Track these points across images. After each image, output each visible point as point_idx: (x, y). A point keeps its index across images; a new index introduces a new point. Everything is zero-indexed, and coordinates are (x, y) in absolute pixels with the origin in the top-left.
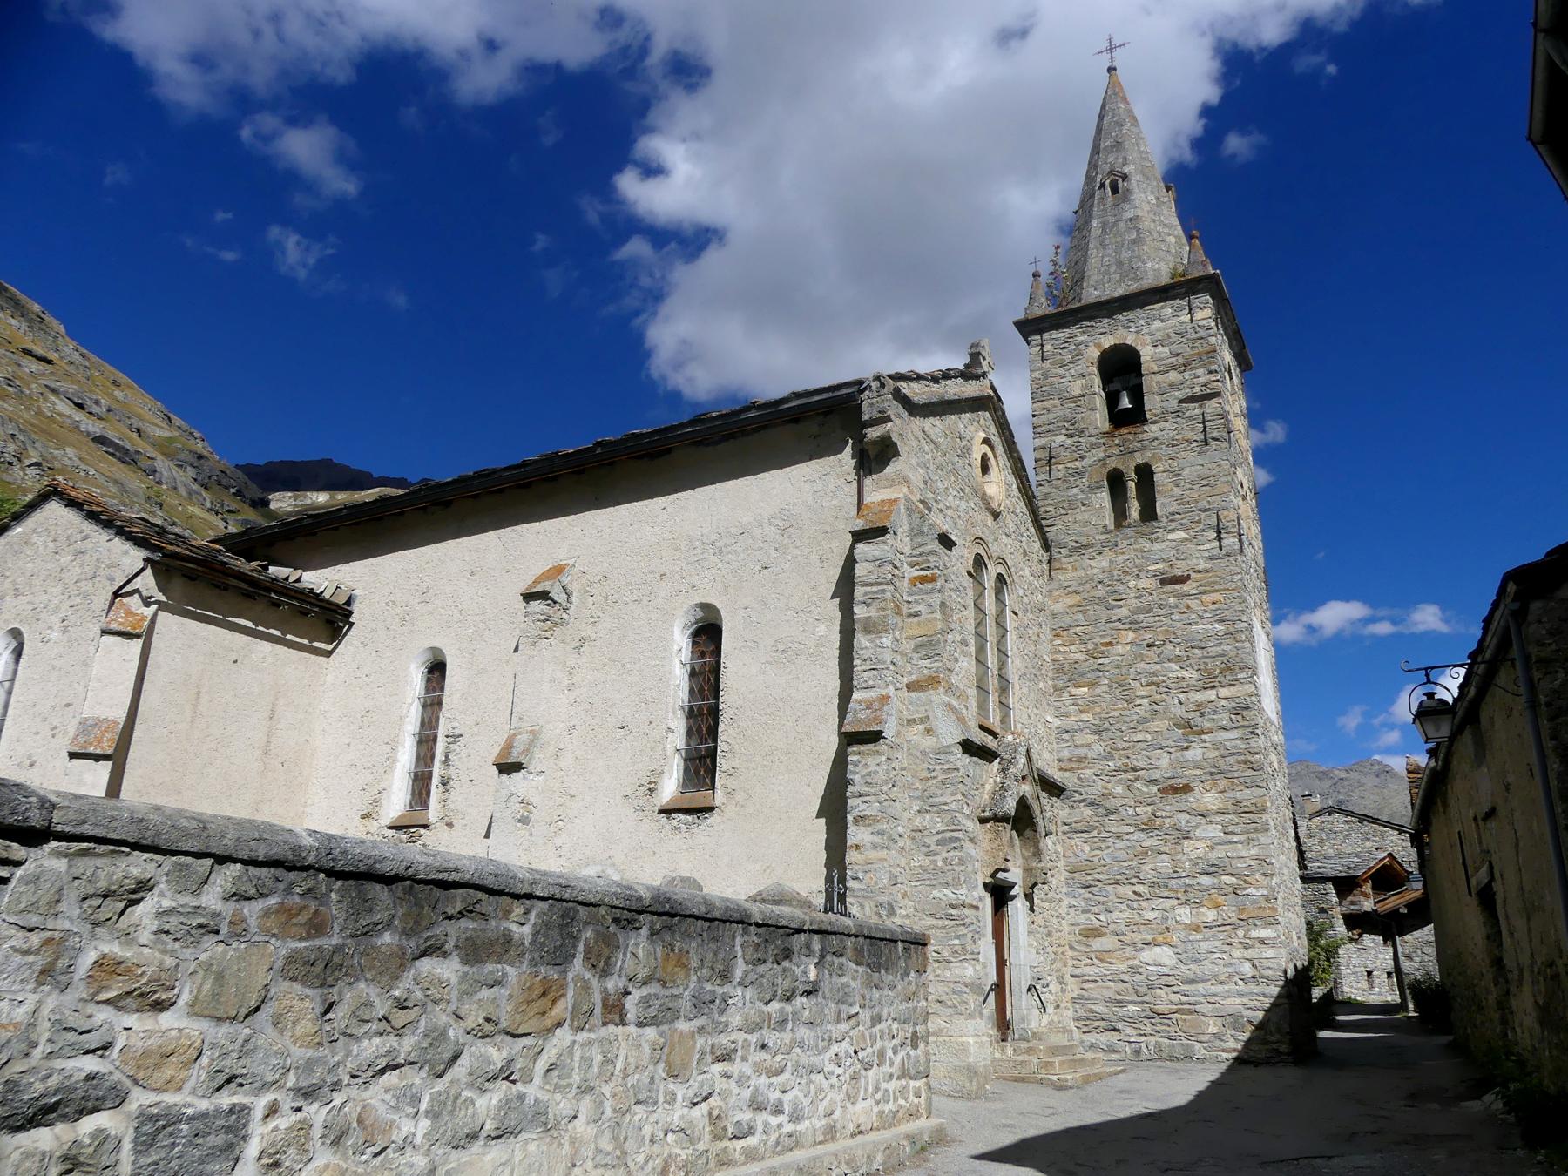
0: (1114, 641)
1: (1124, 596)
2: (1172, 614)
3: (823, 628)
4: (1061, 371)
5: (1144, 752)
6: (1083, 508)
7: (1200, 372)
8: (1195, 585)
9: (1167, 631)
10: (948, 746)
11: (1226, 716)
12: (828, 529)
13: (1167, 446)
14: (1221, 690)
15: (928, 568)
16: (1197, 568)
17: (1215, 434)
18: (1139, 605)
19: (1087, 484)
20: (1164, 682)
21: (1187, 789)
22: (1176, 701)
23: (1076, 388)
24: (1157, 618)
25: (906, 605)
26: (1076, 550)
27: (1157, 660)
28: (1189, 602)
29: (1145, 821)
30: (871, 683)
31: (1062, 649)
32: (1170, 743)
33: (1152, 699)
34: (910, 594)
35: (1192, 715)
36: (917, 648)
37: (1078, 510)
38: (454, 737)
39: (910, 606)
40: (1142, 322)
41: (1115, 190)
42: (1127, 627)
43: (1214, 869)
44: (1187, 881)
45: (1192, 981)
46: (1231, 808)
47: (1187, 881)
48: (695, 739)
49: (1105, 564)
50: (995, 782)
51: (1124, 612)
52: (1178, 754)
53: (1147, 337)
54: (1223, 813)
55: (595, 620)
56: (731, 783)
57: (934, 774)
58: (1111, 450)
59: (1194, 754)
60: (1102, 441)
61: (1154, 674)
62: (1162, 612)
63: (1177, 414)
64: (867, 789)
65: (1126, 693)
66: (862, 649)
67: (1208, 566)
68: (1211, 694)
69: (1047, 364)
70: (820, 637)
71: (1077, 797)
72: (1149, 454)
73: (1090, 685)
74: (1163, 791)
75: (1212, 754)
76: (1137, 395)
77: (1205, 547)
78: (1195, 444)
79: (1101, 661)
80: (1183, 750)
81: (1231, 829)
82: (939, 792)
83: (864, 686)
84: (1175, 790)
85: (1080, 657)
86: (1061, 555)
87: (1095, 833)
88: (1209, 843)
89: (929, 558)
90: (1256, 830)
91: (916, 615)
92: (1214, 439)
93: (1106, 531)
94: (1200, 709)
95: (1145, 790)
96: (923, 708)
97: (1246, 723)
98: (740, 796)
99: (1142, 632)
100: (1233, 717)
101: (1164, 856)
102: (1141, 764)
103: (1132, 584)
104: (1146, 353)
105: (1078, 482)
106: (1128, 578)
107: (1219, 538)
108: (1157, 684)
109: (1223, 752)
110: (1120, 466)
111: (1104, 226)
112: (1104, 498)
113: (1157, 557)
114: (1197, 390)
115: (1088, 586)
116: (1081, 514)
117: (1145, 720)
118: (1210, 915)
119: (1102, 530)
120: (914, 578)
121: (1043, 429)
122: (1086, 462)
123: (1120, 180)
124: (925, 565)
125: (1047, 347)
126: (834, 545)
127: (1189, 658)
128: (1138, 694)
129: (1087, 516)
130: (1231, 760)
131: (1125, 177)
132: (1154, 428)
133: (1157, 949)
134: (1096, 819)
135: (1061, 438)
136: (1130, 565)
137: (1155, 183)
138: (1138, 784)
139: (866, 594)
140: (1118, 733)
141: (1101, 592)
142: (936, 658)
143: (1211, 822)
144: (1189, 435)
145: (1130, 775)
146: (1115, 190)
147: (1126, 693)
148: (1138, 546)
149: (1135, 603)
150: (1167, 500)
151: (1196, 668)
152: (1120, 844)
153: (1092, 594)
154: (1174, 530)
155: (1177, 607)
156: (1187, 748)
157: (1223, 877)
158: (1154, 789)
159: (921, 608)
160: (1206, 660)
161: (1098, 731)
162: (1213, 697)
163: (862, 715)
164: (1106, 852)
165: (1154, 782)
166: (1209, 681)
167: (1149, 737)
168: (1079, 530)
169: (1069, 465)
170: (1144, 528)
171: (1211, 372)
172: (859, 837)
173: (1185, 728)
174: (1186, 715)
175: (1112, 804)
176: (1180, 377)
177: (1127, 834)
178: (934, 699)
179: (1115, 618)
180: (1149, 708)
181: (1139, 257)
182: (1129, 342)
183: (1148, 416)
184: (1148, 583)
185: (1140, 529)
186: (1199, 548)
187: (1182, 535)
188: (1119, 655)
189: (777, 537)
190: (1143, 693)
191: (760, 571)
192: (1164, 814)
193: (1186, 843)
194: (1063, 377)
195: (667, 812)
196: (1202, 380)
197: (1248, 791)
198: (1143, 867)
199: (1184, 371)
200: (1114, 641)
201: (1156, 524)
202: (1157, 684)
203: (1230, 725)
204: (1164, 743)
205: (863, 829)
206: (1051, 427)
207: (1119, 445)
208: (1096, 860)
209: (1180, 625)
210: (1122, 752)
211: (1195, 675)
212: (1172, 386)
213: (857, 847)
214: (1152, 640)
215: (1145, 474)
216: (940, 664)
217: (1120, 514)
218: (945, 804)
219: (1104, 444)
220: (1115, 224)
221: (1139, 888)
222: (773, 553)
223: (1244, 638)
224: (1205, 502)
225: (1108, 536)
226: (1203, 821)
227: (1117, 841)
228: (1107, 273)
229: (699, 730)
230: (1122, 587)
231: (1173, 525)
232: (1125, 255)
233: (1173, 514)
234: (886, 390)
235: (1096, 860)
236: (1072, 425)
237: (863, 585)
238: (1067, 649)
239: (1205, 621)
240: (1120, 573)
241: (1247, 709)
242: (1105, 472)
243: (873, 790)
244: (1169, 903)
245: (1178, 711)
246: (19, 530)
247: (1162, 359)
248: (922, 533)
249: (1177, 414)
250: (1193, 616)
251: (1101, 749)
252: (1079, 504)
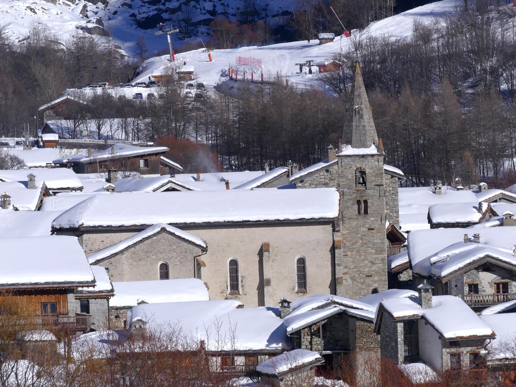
17: (382, 195)
21: (371, 276)
36: (345, 267)
38: (243, 277)
40: (367, 162)
46: (380, 280)
48: (299, 280)
49: (356, 223)
51: (359, 236)
55: (276, 255)
56: (310, 289)
59: (373, 268)
61: (365, 250)
69: (343, 169)
72: (367, 198)
73: (352, 251)
74: (366, 276)
84: (368, 276)
85: (349, 245)
93: (356, 215)
98: (312, 291)
103: (362, 229)
108: (366, 253)
111: (356, 126)
112: (356, 207)
114: (378, 184)
116: (350, 210)
117: (363, 261)
122: (352, 197)
125: (343, 164)
126: (328, 247)
132: (368, 191)
135: (346, 190)
137: (368, 110)
138: (361, 275)
141: (355, 230)
145: (359, 272)
146: (359, 113)
149: (362, 234)
154: (372, 217)
158: (364, 276)
159: (345, 260)
161: (353, 262)
175: (356, 279)
181: (366, 140)
184: (365, 229)
190: (363, 254)
195: (297, 293)
196: (380, 181)
202: (366, 253)
211: (374, 251)
215: (366, 202)
217: (359, 213)
220: (359, 127)
221: (361, 297)
228: (358, 143)
229: (300, 278)
231: (371, 216)
232: (363, 139)
245: (370, 259)
246: (155, 238)
247: (371, 173)
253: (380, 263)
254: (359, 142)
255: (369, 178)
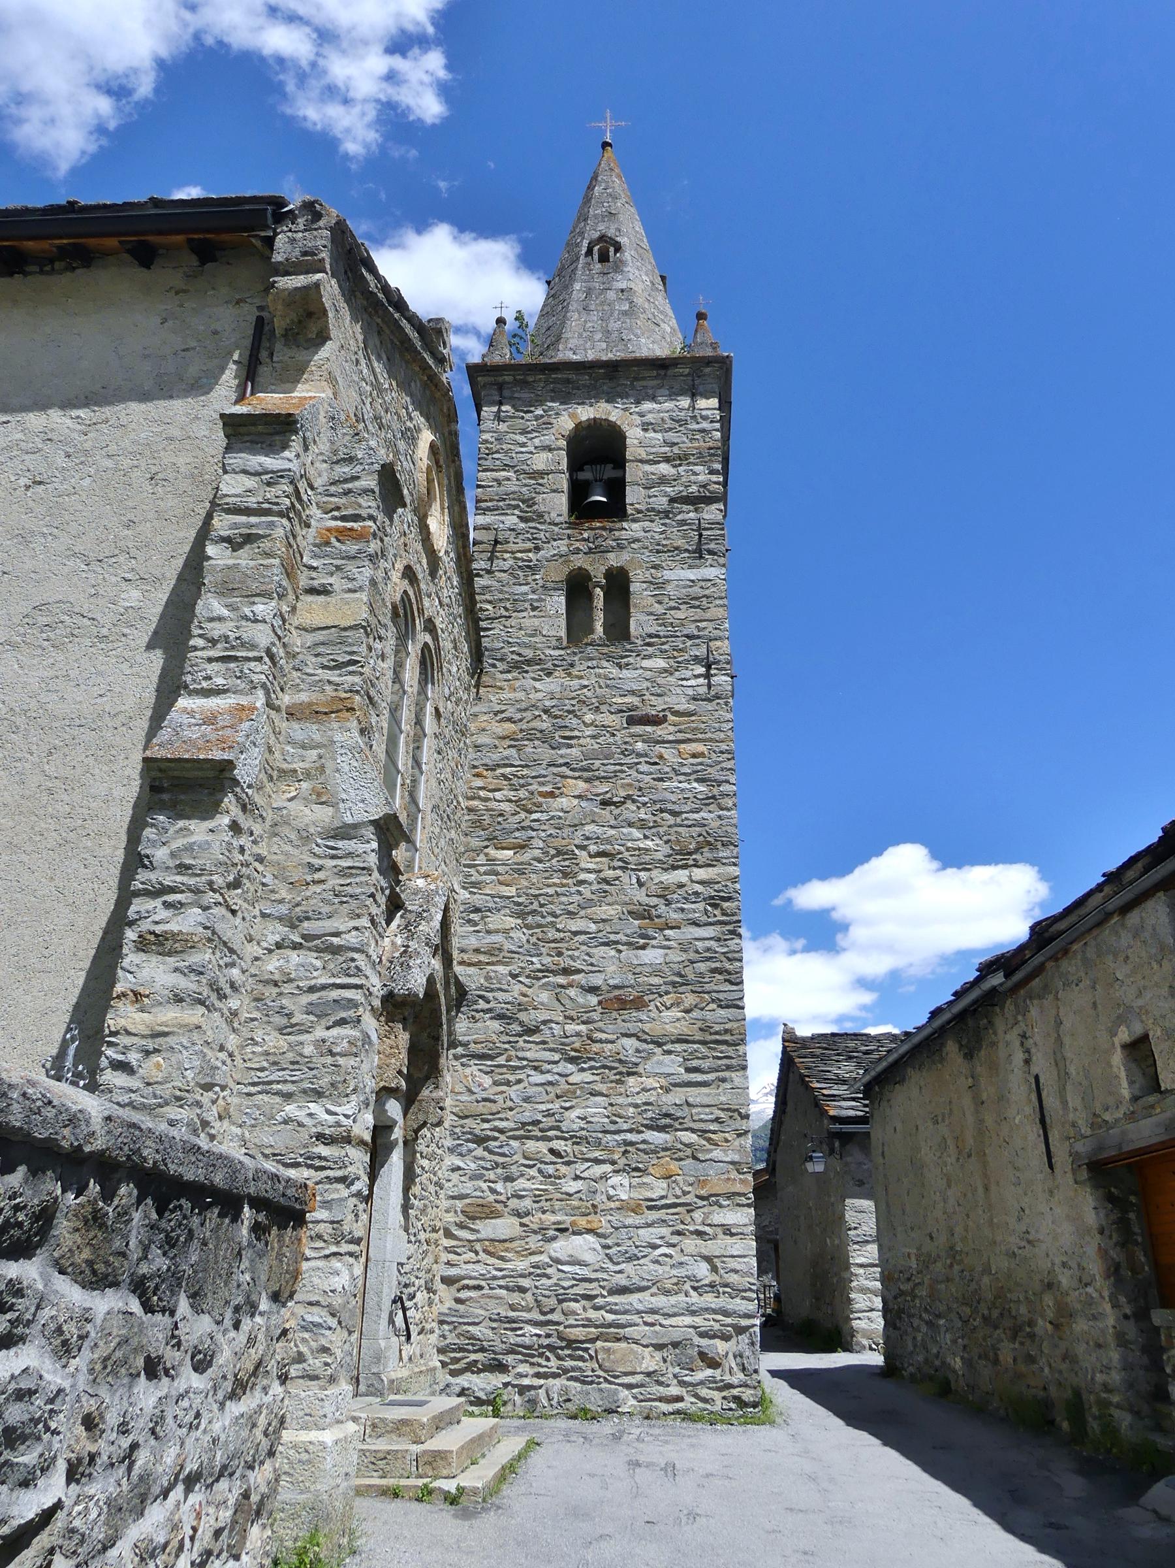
0: (557, 792)
1: (576, 733)
2: (640, 763)
3: (135, 594)
4: (522, 439)
5: (584, 948)
6: (532, 614)
7: (698, 469)
8: (672, 728)
9: (630, 785)
10: (355, 826)
11: (701, 906)
12: (176, 433)
13: (651, 551)
14: (695, 869)
15: (356, 518)
16: (677, 708)
17: (712, 546)
18: (596, 746)
19: (541, 582)
20: (621, 853)
21: (639, 1004)
22: (634, 881)
23: (541, 461)
24: (618, 768)
25: (306, 572)
26: (516, 666)
27: (613, 822)
28: (663, 750)
29: (577, 1045)
30: (220, 681)
31: (482, 793)
32: (621, 937)
33: (602, 875)
34: (315, 556)
35: (654, 901)
37: (524, 614)
39: (314, 574)
41: (604, 258)
42: (577, 774)
43: (668, 1121)
44: (630, 1137)
45: (623, 1290)
47: (630, 1137)
50: (393, 943)
52: (632, 953)
53: (635, 417)
54: (687, 1041)
57: (317, 876)
58: (578, 544)
59: (653, 956)
60: (569, 531)
61: (608, 841)
62: (628, 760)
63: (666, 514)
64: (179, 878)
65: (567, 863)
66: (211, 620)
67: (692, 707)
68: (681, 876)
69: (503, 427)
70: (126, 609)
71: (482, 1005)
75: (676, 956)
76: (617, 489)
77: (692, 682)
78: (686, 555)
79: (535, 816)
80: (638, 948)
81: (695, 1063)
82: (326, 909)
83: (205, 684)
84: (622, 1004)
85: (505, 806)
86: (495, 674)
87: (501, 1060)
88: (663, 1082)
89: (360, 500)
90: (729, 1068)
91: (324, 591)
92: (711, 552)
94: (664, 894)
95: (581, 1000)
96: (314, 753)
97: (725, 918)
99: (597, 783)
100: (709, 908)
101: (599, 1099)
102: (577, 965)
104: (634, 435)
105: (530, 579)
106: (585, 710)
107: (708, 676)
109: (692, 956)
110: (588, 568)
111: (589, 292)
112: (558, 602)
113: (626, 687)
114: (694, 489)
115: (528, 715)
117: (590, 903)
118: (659, 1188)
119: (554, 643)
120: (329, 530)
121: (489, 504)
123: (612, 249)
124: (350, 512)
127: (656, 825)
128: (583, 865)
129: (536, 622)
130: (702, 967)
131: (618, 248)
132: (635, 526)
133: (577, 1239)
134: (505, 1038)
135: (512, 520)
136: (589, 694)
138: (572, 992)
139: (235, 526)
140: (550, 919)
141: (545, 724)
142: (351, 668)
143: (669, 1052)
144: (680, 543)
145: (561, 980)
146: (604, 258)
147: (567, 863)
148: (601, 671)
150: (644, 618)
151: (665, 838)
152: (538, 1078)
153: (534, 724)
154: (650, 657)
155: (646, 755)
156: (643, 947)
157: (679, 1133)
160: (680, 829)
162: (684, 880)
163: (194, 734)
164: (515, 1088)
165: (593, 990)
166: (681, 857)
167: (593, 927)
168: (526, 640)
169: (519, 555)
170: (612, 649)
171: (712, 472)
172: (145, 974)
173: (645, 918)
174: (646, 900)
176: (673, 471)
177: (550, 1063)
178: (338, 737)
179: (561, 761)
180: (595, 887)
181: (630, 329)
182: (612, 419)
183: (630, 510)
185: (605, 650)
186: (680, 683)
187: (661, 663)
188: (562, 810)
189: (75, 435)
191: (28, 487)
192: (603, 1036)
193: (631, 1080)
194: (523, 445)
196: (701, 478)
197: (722, 1012)
198: (567, 1114)
199: (680, 465)
200: (557, 792)
201: (628, 647)
203: (704, 919)
204: (613, 937)
205: (155, 959)
206: (501, 504)
207: (587, 540)
208: (500, 1098)
209: (647, 778)
210: (553, 945)
212: (663, 480)
213: (137, 996)
214: (609, 795)
215: (618, 583)
216: (357, 679)
218: (337, 934)
219: (569, 537)
221: (558, 1145)
222: (61, 461)
223: (730, 804)
224: (693, 626)
225: (562, 652)
226: (658, 1050)
227: (532, 1073)
228: (590, 338)
230: (575, 721)
232: (614, 325)
233: (650, 636)
234: (321, 223)
235: (500, 1098)
236: (528, 506)
237: (229, 511)
238: (490, 795)
239: (682, 778)
240: (573, 702)
241: (729, 899)
242: (566, 571)
243: (192, 881)
244: (598, 1170)
248: (350, 460)
249: (666, 514)
250: (667, 769)
251: (524, 939)
252: (527, 605)
253: (695, 924)
254: (598, 336)
255: (647, 468)
